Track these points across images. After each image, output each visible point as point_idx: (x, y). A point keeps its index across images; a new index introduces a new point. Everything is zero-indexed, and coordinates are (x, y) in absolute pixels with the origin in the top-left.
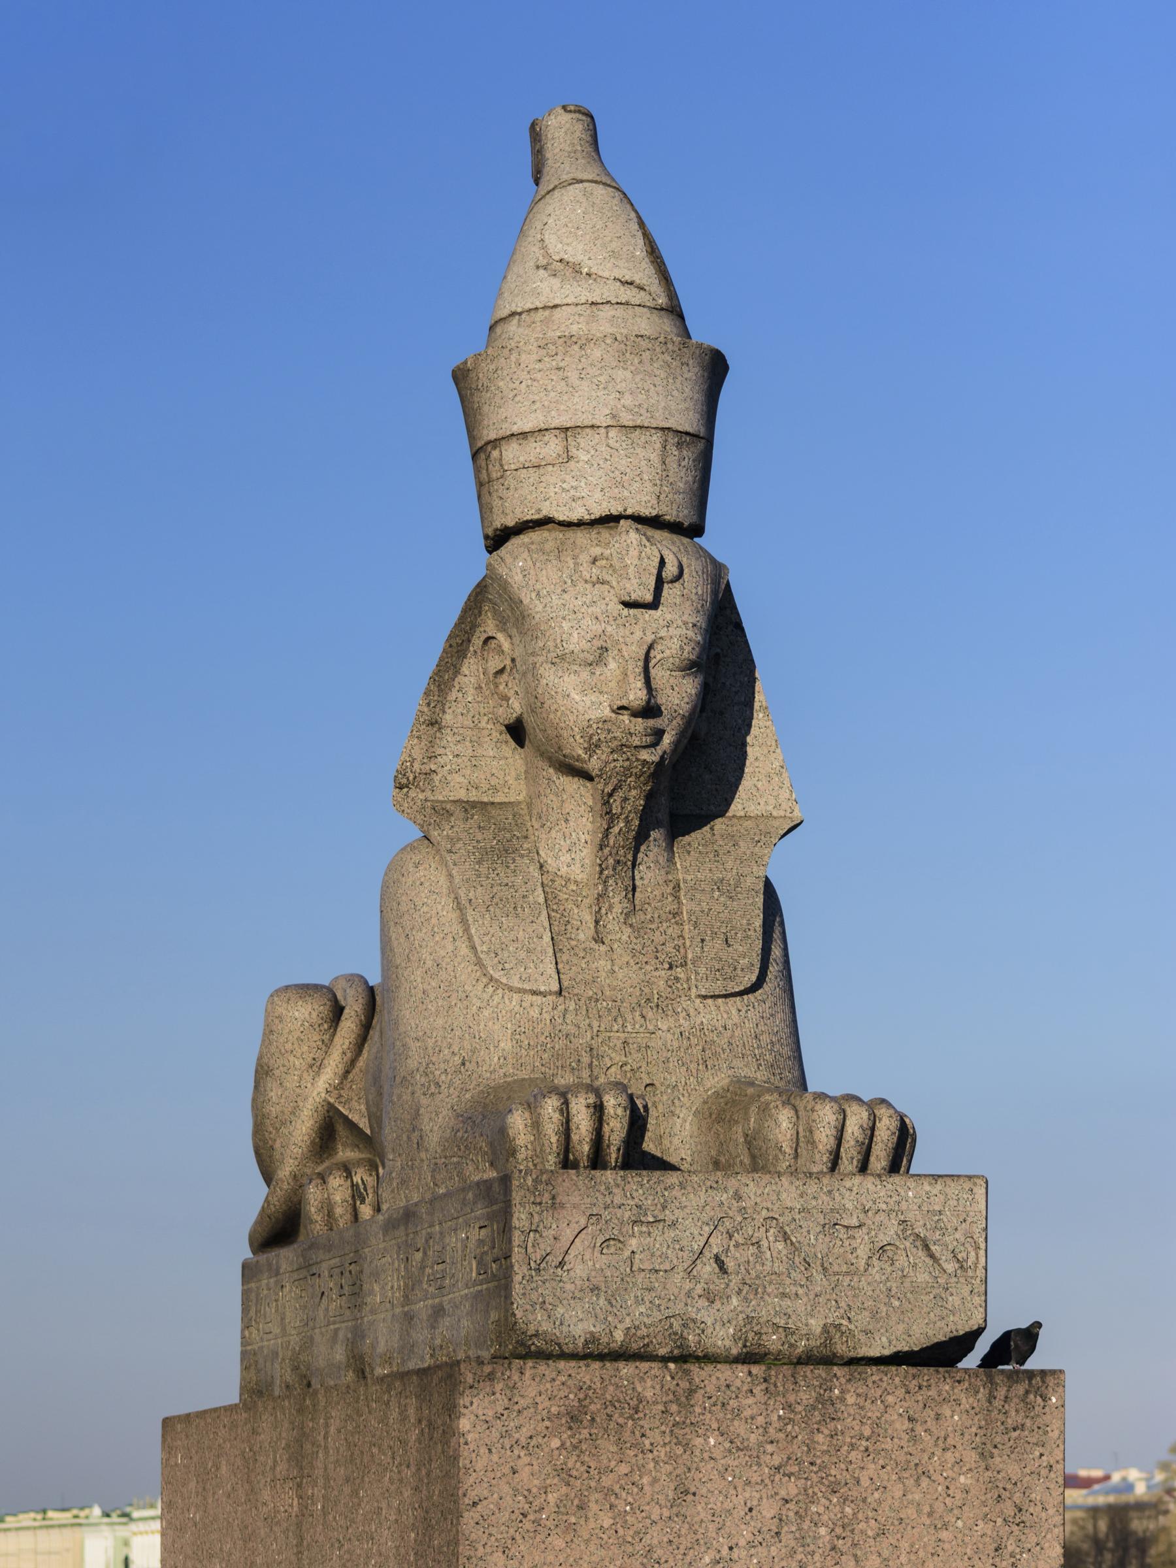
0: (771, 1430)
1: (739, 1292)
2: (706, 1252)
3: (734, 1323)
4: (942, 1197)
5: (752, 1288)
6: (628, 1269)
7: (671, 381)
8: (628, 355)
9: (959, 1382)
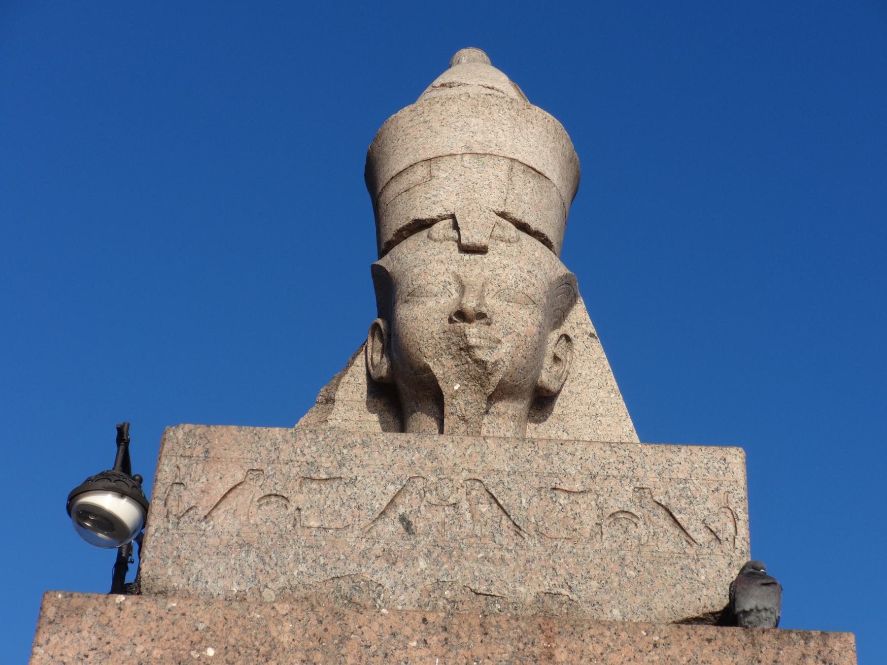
1: (428, 554)
2: (393, 515)
3: (420, 587)
4: (688, 466)
5: (445, 549)
6: (289, 526)
7: (517, 130)
8: (479, 108)
9: (709, 641)
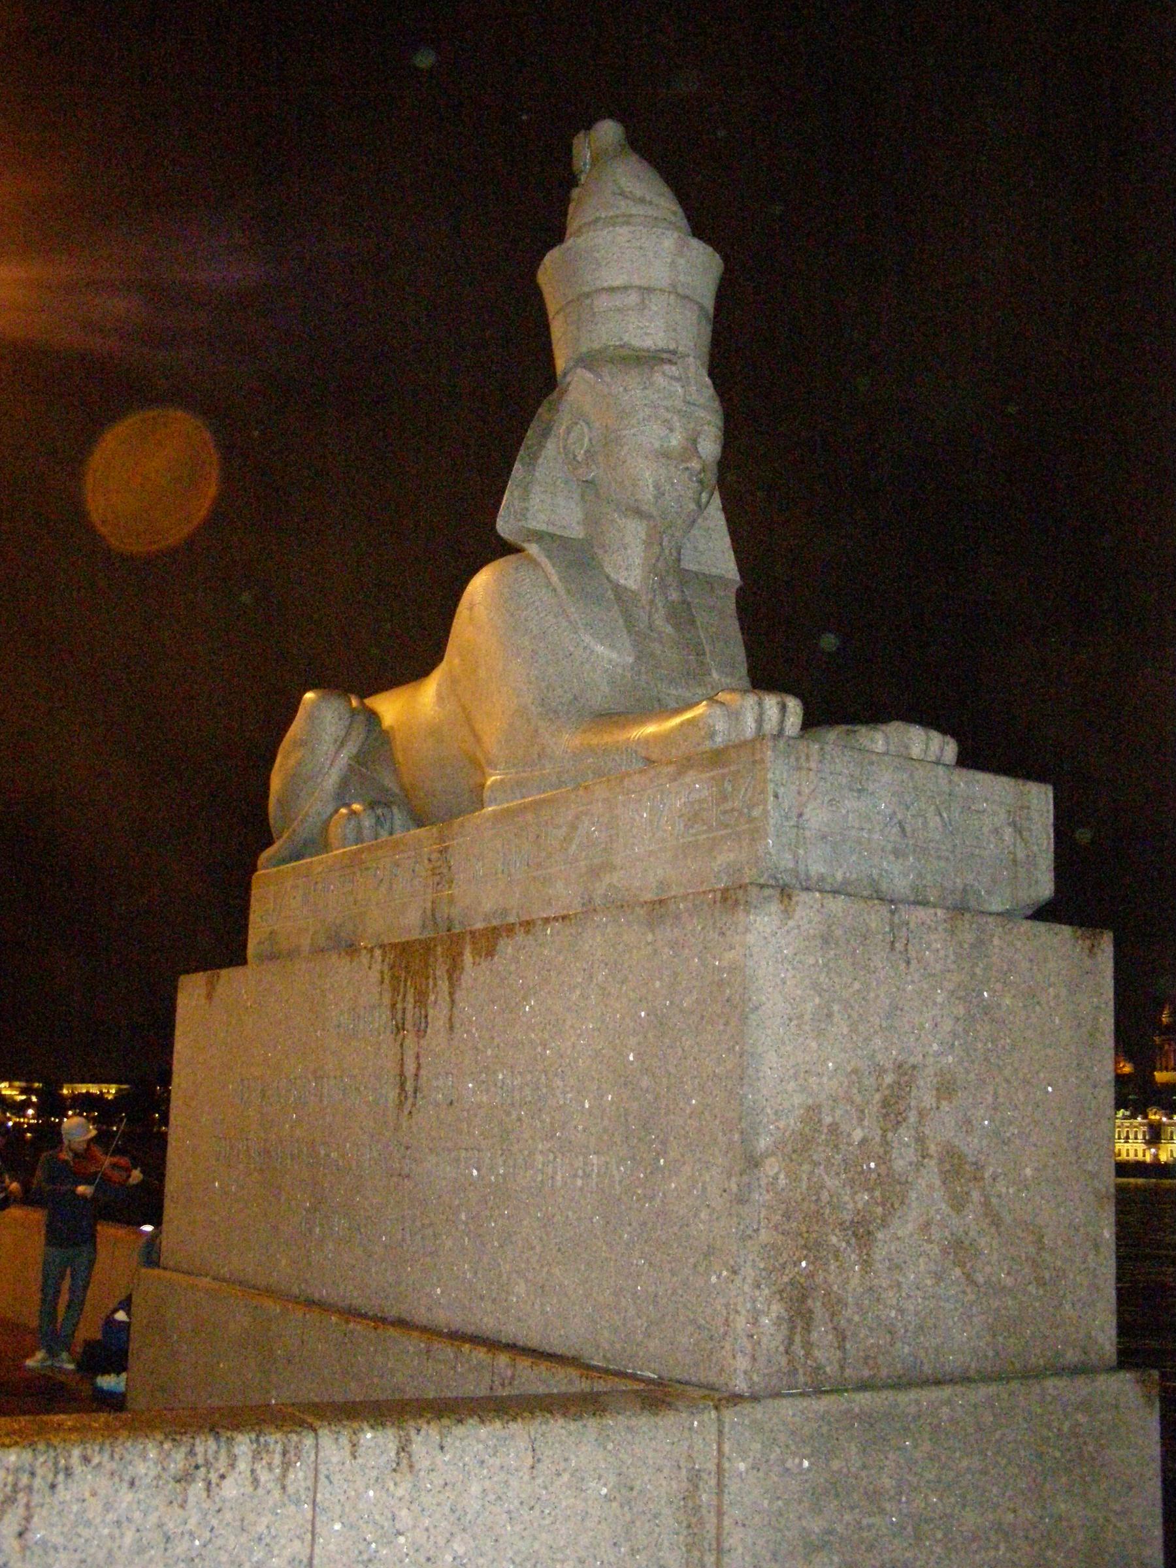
0: (949, 961)
